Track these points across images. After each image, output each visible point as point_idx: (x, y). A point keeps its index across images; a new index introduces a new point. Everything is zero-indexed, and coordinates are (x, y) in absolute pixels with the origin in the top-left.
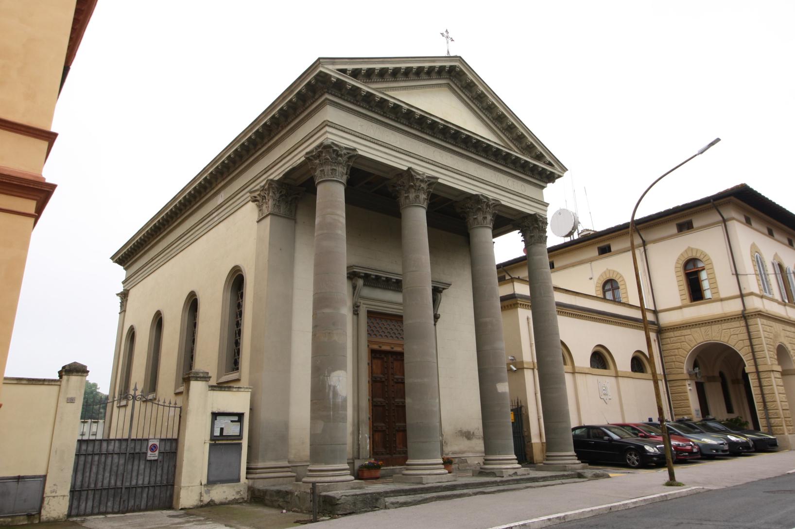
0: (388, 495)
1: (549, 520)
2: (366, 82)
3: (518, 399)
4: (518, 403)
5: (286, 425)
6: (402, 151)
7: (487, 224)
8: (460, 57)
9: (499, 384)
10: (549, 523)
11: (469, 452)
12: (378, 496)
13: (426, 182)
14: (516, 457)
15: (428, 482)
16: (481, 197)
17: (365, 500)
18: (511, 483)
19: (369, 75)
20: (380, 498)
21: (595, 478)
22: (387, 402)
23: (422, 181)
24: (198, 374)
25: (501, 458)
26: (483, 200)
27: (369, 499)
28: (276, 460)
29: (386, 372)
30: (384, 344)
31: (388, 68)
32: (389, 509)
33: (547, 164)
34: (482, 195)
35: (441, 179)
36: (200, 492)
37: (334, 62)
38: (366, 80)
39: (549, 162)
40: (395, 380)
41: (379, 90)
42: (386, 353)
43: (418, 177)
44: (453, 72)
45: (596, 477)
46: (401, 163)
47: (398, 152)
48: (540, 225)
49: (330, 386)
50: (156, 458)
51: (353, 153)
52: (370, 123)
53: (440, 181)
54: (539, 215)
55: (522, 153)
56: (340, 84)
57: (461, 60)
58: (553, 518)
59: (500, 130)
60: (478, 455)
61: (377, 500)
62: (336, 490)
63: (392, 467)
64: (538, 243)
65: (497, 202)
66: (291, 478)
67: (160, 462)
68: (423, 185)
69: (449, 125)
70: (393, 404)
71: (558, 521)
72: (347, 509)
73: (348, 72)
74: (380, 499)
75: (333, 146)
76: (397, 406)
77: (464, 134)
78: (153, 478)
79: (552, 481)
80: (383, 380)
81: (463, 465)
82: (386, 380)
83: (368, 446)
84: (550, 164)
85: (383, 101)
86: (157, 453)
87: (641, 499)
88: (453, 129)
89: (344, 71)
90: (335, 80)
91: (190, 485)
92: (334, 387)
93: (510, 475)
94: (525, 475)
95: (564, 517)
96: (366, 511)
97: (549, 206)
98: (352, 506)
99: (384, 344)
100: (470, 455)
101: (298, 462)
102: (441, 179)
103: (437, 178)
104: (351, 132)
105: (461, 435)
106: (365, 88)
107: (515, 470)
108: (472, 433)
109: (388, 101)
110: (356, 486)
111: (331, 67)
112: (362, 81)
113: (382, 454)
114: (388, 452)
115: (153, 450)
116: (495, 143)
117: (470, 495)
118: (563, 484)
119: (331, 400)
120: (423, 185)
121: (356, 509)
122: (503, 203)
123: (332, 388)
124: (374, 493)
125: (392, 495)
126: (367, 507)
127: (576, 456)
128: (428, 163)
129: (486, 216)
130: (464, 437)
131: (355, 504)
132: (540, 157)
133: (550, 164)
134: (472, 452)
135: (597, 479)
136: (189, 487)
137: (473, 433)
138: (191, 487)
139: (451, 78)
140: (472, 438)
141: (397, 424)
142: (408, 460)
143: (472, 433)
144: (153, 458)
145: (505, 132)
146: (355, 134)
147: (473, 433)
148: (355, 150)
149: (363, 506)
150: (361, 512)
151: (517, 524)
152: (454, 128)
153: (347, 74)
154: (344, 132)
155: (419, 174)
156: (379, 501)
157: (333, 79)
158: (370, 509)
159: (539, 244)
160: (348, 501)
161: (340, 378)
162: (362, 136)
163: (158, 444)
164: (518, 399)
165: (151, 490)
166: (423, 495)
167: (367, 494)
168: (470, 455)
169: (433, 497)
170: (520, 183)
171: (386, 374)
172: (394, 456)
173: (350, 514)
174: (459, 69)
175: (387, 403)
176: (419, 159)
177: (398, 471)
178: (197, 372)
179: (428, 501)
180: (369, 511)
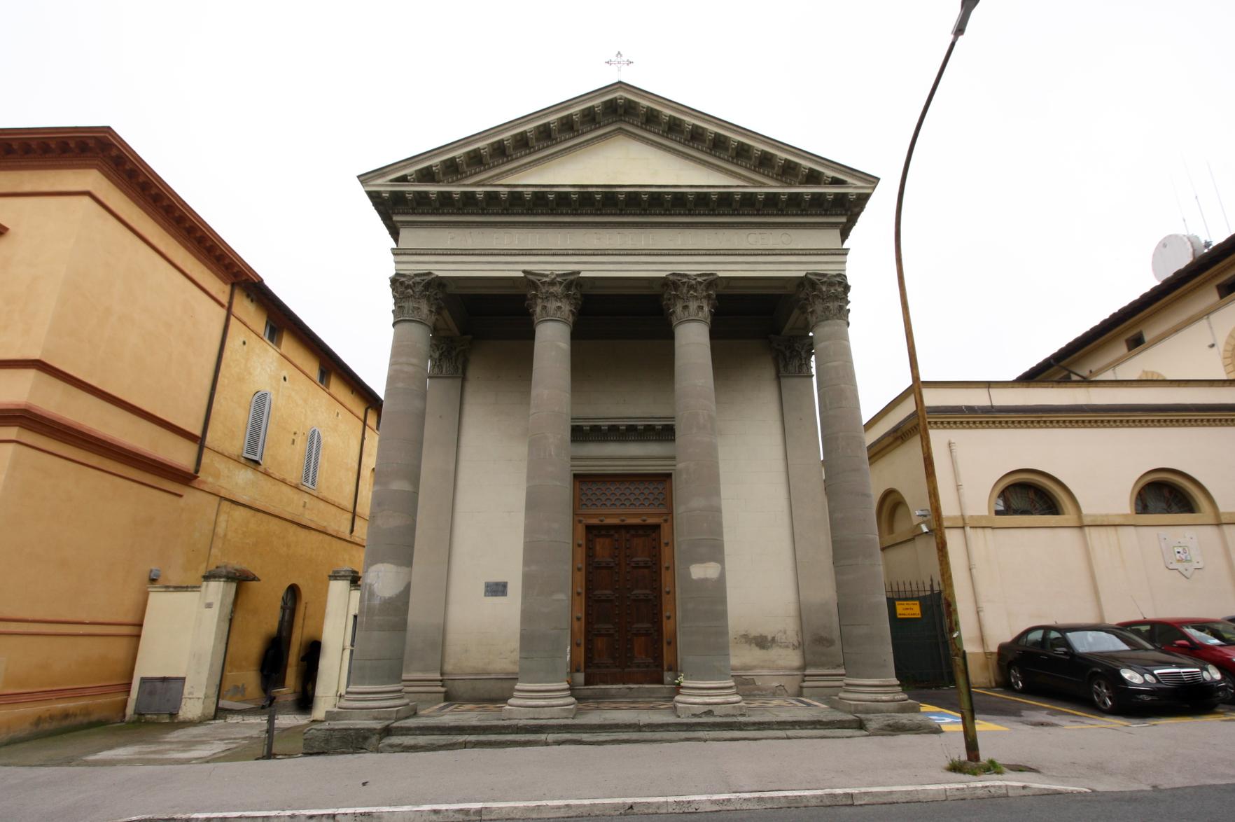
0: (411, 732)
1: (436, 812)
2: (457, 180)
3: (932, 580)
4: (932, 586)
5: (443, 631)
8: (620, 82)
11: (762, 668)
13: (560, 283)
14: (899, 682)
15: (511, 717)
16: (671, 278)
17: (344, 738)
18: (671, 729)
19: (452, 169)
23: (552, 283)
24: (338, 573)
25: (691, 685)
26: (679, 283)
27: (351, 736)
28: (425, 670)
30: (607, 516)
31: (479, 148)
32: (381, 752)
33: (831, 183)
34: (674, 274)
37: (384, 173)
39: (833, 178)
40: (633, 565)
41: (482, 183)
43: (545, 279)
44: (619, 110)
45: (893, 731)
46: (512, 269)
48: (824, 289)
49: (366, 584)
51: (428, 278)
53: (582, 275)
54: (816, 274)
55: (786, 183)
56: (422, 198)
58: (447, 810)
59: (728, 161)
60: (781, 673)
61: (366, 738)
62: (350, 720)
64: (823, 321)
65: (711, 277)
66: (438, 694)
68: (553, 289)
70: (628, 597)
71: (460, 817)
73: (409, 178)
74: (371, 738)
75: (398, 278)
77: (621, 193)
79: (780, 732)
80: (612, 565)
81: (743, 687)
82: (616, 565)
83: (568, 657)
84: (836, 182)
85: (492, 198)
87: (757, 795)
88: (598, 193)
89: (403, 179)
90: (387, 195)
93: (694, 715)
94: (733, 716)
96: (343, 753)
97: (850, 253)
98: (322, 745)
99: (607, 516)
100: (765, 672)
103: (579, 272)
104: (429, 252)
106: (456, 189)
107: (710, 708)
108: (769, 638)
109: (473, 193)
111: (380, 181)
112: (445, 181)
113: (608, 667)
114: (617, 664)
117: (546, 744)
118: (788, 738)
120: (553, 289)
122: (721, 274)
123: (368, 587)
124: (363, 729)
125: (418, 732)
127: (899, 685)
128: (567, 255)
129: (687, 304)
130: (753, 645)
131: (327, 741)
132: (813, 177)
134: (769, 668)
135: (893, 735)
137: (773, 639)
140: (771, 646)
141: (635, 626)
143: (769, 638)
145: (738, 160)
146: (437, 252)
147: (773, 639)
148: (430, 274)
149: (341, 746)
150: (335, 753)
152: (600, 190)
153: (408, 182)
155: (546, 276)
156: (370, 741)
157: (384, 195)
158: (351, 750)
159: (826, 322)
160: (317, 736)
161: (380, 574)
162: (449, 252)
164: (932, 580)
166: (450, 737)
167: (351, 729)
168: (765, 672)
171: (616, 556)
172: (626, 670)
173: (318, 754)
174: (622, 101)
177: (613, 692)
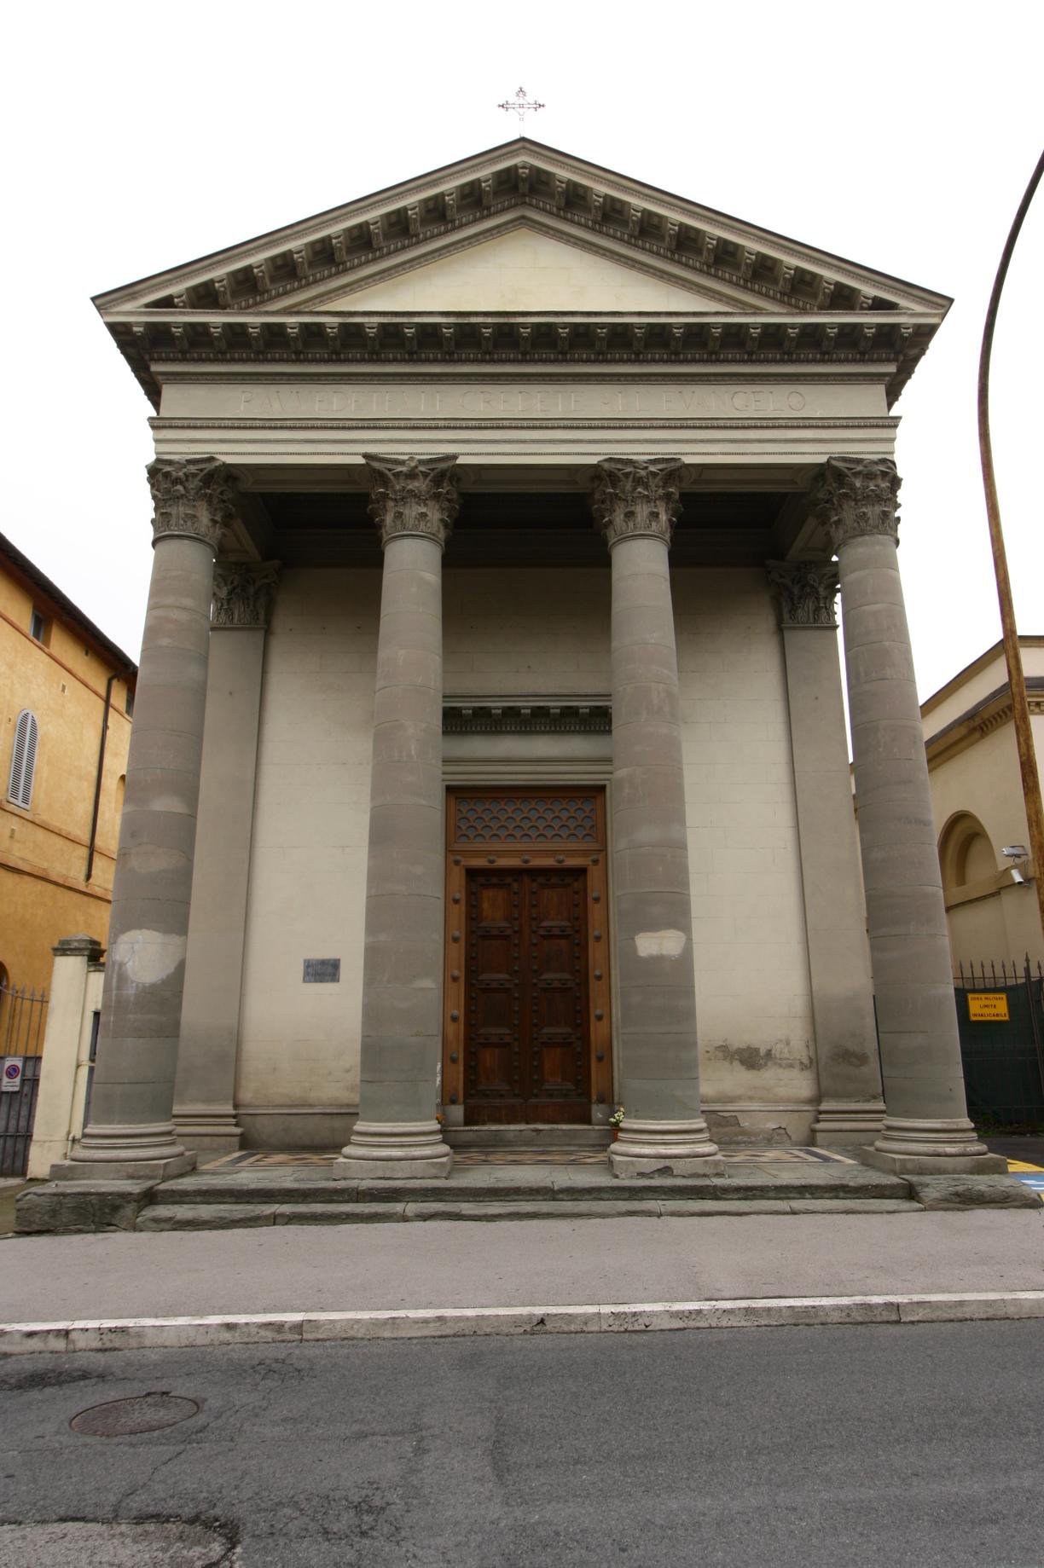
0: (187, 1199)
1: (230, 1327)
2: (256, 304)
3: (1027, 960)
4: (1027, 970)
5: (237, 1038)
6: (354, 424)
7: (635, 528)
8: (523, 139)
9: (641, 935)
10: (227, 1336)
11: (751, 1099)
12: (118, 1202)
13: (425, 475)
14: (973, 1125)
15: (348, 1175)
16: (606, 466)
17: (81, 1208)
18: (605, 1196)
19: (247, 285)
20: (125, 1205)
21: (961, 1206)
22: (517, 981)
23: (412, 475)
24: (70, 944)
25: (636, 1127)
26: (619, 474)
27: (92, 1205)
28: (208, 1100)
29: (516, 916)
30: (500, 853)
31: (290, 251)
32: (141, 1231)
33: (870, 308)
34: (610, 460)
35: (463, 454)
36: (65, 1151)
37: (135, 293)
38: (254, 298)
39: (875, 299)
40: (542, 932)
41: (295, 309)
42: (515, 873)
43: (400, 469)
44: (521, 185)
45: (963, 1202)
46: (345, 452)
47: (344, 428)
48: (858, 484)
49: (114, 963)
50: (17, 1089)
51: (210, 466)
52: (273, 388)
53: (460, 461)
54: (844, 460)
55: (797, 307)
56: (198, 333)
57: (528, 146)
58: (247, 1324)
59: (701, 271)
60: (781, 1108)
61: (115, 1209)
62: (89, 1178)
63: (494, 1127)
64: (854, 537)
65: (672, 464)
66: (229, 1138)
67: (26, 1095)
68: (414, 485)
69: (473, 320)
70: (535, 985)
71: (268, 1335)
72: (34, 1222)
73: (176, 300)
74: (123, 1207)
75: (160, 467)
76: (482, 990)
77: (524, 326)
78: (13, 1122)
79: (779, 1202)
80: (508, 932)
81: (721, 1130)
82: (516, 932)
83: (439, 1079)
84: (880, 305)
85: (313, 333)
86: (18, 1080)
87: (743, 1304)
88: (486, 326)
89: (167, 303)
90: (141, 329)
91: (46, 1138)
92: (121, 965)
93: (641, 1175)
94: (705, 1176)
95: (298, 1327)
96: (80, 1232)
97: (902, 424)
98: (46, 1217)
99: (500, 853)
100: (755, 1106)
101: (315, 1106)
102: (463, 454)
103: (455, 457)
104: (210, 423)
105: (725, 1058)
106: (253, 319)
107: (667, 1162)
108: (763, 1052)
109: (282, 326)
110: (141, 1174)
111: (128, 307)
112: (236, 306)
113: (502, 1096)
114: (517, 1091)
115: (12, 1075)
116: (717, 314)
117: (404, 1218)
118: (794, 1213)
119: (114, 992)
120: (414, 485)
121: (58, 1223)
122: (688, 460)
123: (116, 967)
124: (110, 1194)
125: (198, 1199)
126: (85, 1224)
127: (973, 1130)
128: (437, 428)
129: (632, 509)
130: (736, 1064)
131: (54, 1213)
132: (843, 298)
133: (880, 305)
134: (761, 1099)
135: (963, 1210)
136: (44, 1142)
137: (769, 1054)
138: (47, 1144)
139: (527, 199)
140: (766, 1065)
141: (546, 1030)
142: (822, 1104)
143: (763, 1052)
144: (11, 1089)
145: (717, 270)
146: (223, 423)
147: (769, 1054)
148: (211, 459)
149: (76, 1220)
150: (67, 1231)
151: (92, 1324)
152: (489, 320)
153: (176, 307)
154: (195, 428)
155: (402, 463)
156: (122, 1212)
157: (135, 329)
158: (93, 1227)
159: (860, 539)
160: (37, 1206)
161: (136, 947)
162: (242, 424)
163: (20, 1065)
164: (1027, 960)
165: (10, 1142)
166: (250, 1207)
167: (92, 1194)
168: (755, 1106)
169: (282, 1215)
170: (747, 390)
171: (516, 919)
172: (533, 1100)
173: (39, 1233)
174: (527, 171)
175: (516, 985)
176: (406, 428)
177: (510, 1136)
178: (67, 941)
179: (260, 1222)
180: (88, 1232)
